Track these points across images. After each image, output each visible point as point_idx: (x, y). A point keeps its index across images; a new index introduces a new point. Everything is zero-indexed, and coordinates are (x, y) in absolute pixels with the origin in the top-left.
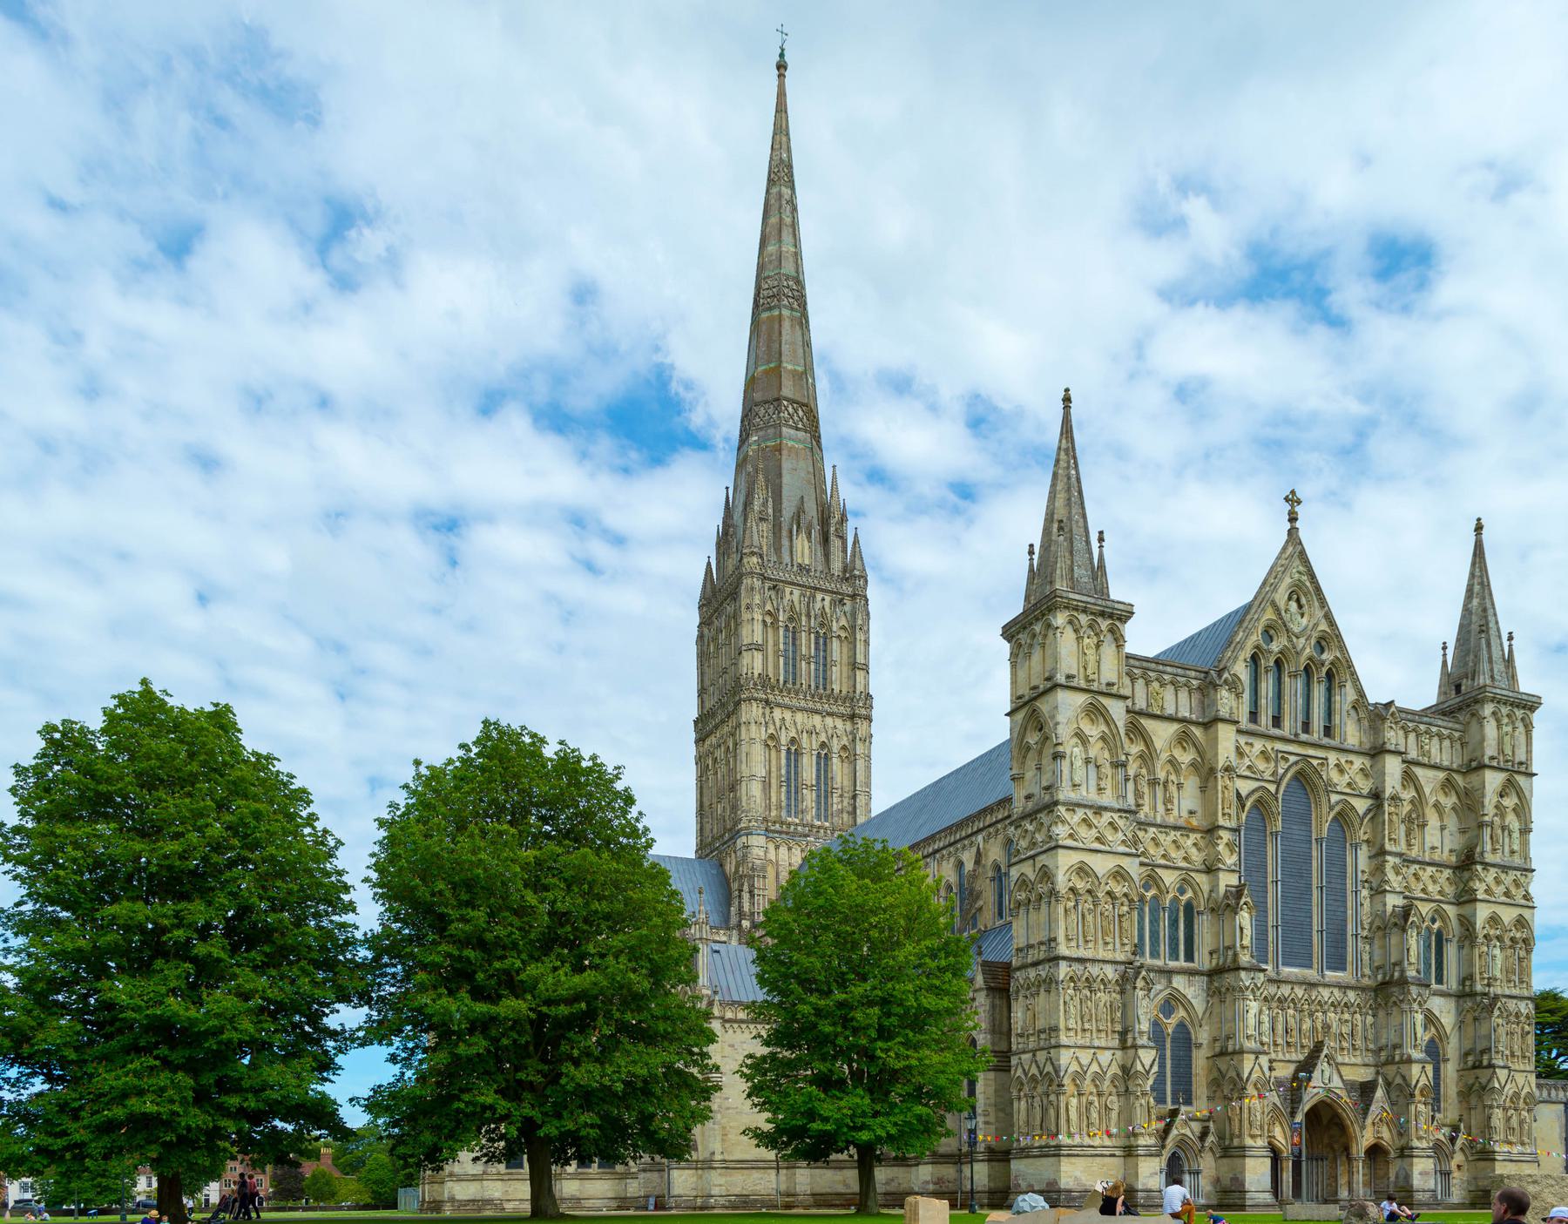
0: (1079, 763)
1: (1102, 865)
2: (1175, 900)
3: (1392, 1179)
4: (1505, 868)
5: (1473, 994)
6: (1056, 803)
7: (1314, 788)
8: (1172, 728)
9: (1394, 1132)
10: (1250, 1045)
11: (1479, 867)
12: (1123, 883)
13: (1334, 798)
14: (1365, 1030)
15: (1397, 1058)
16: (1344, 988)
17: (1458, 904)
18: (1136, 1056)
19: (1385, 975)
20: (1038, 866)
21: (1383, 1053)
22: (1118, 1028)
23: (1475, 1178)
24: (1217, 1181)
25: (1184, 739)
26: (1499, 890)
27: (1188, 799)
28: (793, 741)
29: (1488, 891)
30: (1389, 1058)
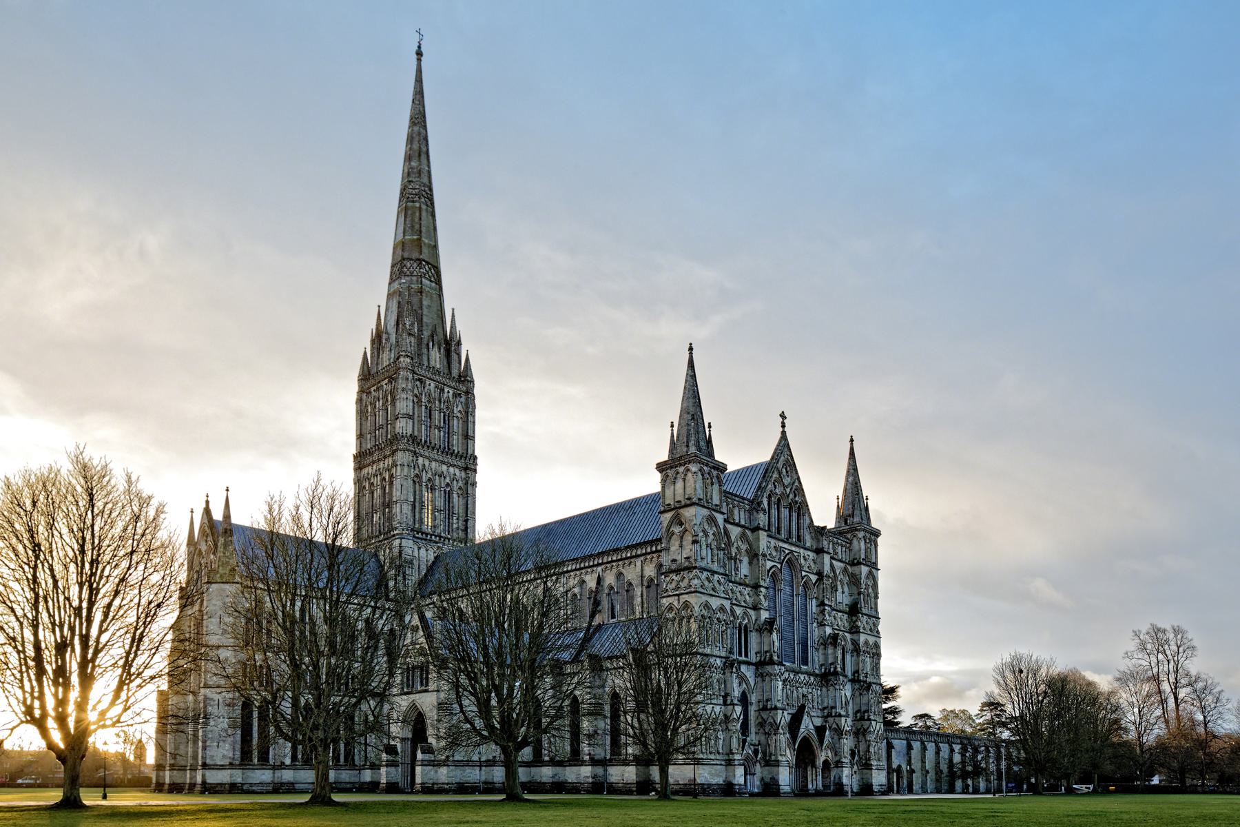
2: (740, 625)
3: (832, 779)
4: (870, 616)
5: (859, 681)
8: (739, 530)
10: (779, 705)
13: (804, 574)
16: (809, 674)
17: (850, 633)
19: (826, 669)
20: (682, 601)
21: (826, 711)
22: (723, 694)
24: (762, 779)
25: (743, 537)
26: (868, 627)
27: (744, 569)
30: (829, 713)
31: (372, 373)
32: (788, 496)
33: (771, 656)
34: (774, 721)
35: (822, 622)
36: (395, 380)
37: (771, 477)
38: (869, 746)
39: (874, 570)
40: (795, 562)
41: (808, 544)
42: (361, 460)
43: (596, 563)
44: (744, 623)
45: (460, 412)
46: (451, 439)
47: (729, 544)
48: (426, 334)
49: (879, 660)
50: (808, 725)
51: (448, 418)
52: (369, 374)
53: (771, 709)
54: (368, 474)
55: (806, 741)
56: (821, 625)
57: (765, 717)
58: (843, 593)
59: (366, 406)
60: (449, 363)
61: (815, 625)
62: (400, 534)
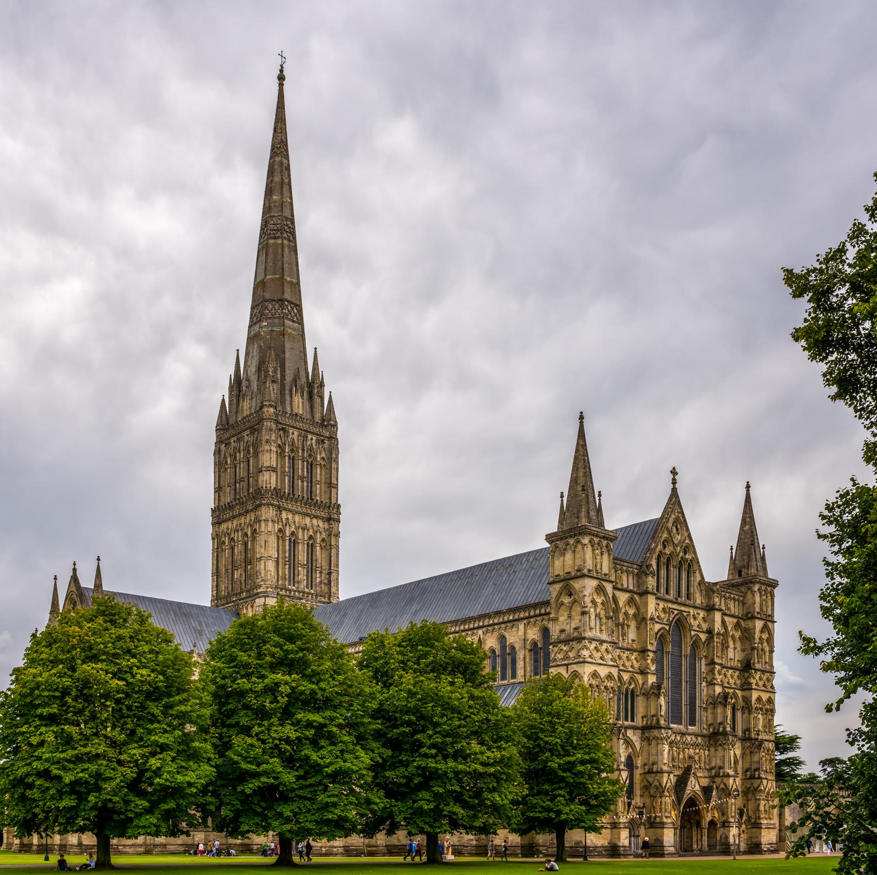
0: (593, 617)
1: (603, 672)
2: (627, 690)
3: (718, 838)
4: (763, 672)
5: (750, 739)
6: (584, 638)
7: (684, 627)
9: (720, 813)
10: (665, 768)
11: (753, 671)
12: (610, 681)
13: (693, 633)
14: (705, 758)
16: (696, 735)
17: (742, 690)
18: (620, 775)
19: (714, 729)
21: (713, 771)
23: (751, 838)
25: (631, 602)
26: (761, 683)
27: (632, 634)
28: (293, 534)
29: (757, 684)
32: (678, 555)
33: (658, 720)
34: (660, 784)
35: (712, 681)
36: (259, 431)
37: (661, 537)
40: (685, 622)
41: (698, 602)
42: (219, 515)
43: (476, 625)
44: (631, 687)
45: (323, 459)
46: (314, 489)
47: (617, 610)
48: (289, 378)
49: (773, 716)
50: (694, 786)
51: (311, 467)
52: (228, 423)
53: (657, 772)
54: (228, 529)
55: (692, 802)
56: (711, 684)
57: (651, 780)
58: (735, 648)
59: (225, 457)
60: (312, 408)
61: (704, 684)
62: (265, 592)
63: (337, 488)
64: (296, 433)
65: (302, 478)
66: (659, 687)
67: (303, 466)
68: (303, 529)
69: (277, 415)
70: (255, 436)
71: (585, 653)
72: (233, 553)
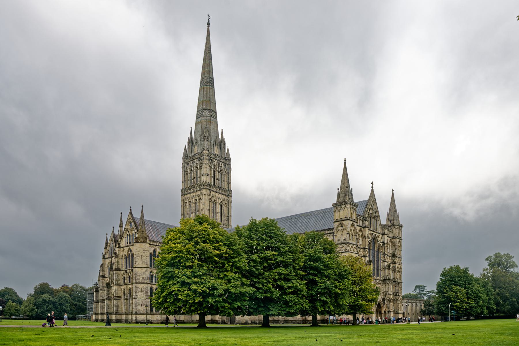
7: (376, 240)
15: (388, 294)
25: (361, 230)
31: (189, 156)
35: (384, 260)
38: (398, 305)
39: (401, 240)
45: (225, 172)
48: (213, 140)
52: (187, 156)
54: (188, 197)
58: (390, 249)
63: (231, 184)
64: (216, 162)
65: (218, 179)
66: (370, 262)
67: (218, 174)
68: (219, 199)
69: (209, 154)
70: (200, 161)
71: (348, 248)
72: (190, 207)
